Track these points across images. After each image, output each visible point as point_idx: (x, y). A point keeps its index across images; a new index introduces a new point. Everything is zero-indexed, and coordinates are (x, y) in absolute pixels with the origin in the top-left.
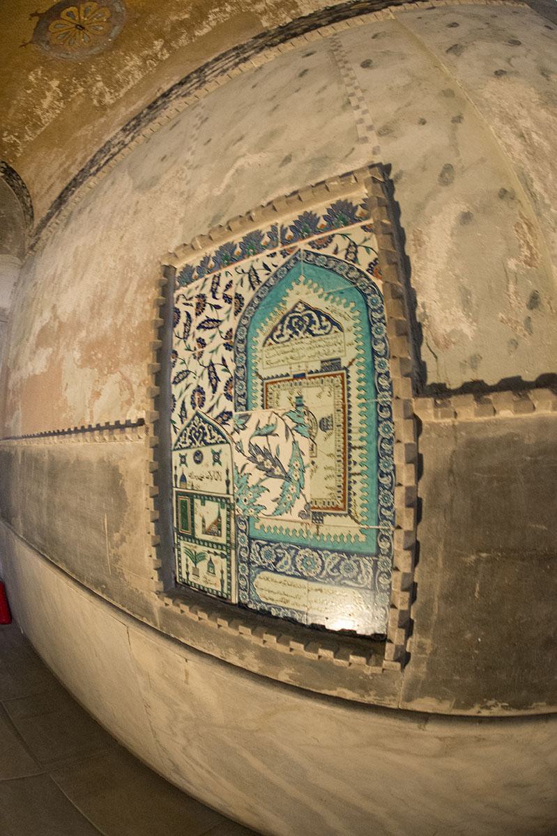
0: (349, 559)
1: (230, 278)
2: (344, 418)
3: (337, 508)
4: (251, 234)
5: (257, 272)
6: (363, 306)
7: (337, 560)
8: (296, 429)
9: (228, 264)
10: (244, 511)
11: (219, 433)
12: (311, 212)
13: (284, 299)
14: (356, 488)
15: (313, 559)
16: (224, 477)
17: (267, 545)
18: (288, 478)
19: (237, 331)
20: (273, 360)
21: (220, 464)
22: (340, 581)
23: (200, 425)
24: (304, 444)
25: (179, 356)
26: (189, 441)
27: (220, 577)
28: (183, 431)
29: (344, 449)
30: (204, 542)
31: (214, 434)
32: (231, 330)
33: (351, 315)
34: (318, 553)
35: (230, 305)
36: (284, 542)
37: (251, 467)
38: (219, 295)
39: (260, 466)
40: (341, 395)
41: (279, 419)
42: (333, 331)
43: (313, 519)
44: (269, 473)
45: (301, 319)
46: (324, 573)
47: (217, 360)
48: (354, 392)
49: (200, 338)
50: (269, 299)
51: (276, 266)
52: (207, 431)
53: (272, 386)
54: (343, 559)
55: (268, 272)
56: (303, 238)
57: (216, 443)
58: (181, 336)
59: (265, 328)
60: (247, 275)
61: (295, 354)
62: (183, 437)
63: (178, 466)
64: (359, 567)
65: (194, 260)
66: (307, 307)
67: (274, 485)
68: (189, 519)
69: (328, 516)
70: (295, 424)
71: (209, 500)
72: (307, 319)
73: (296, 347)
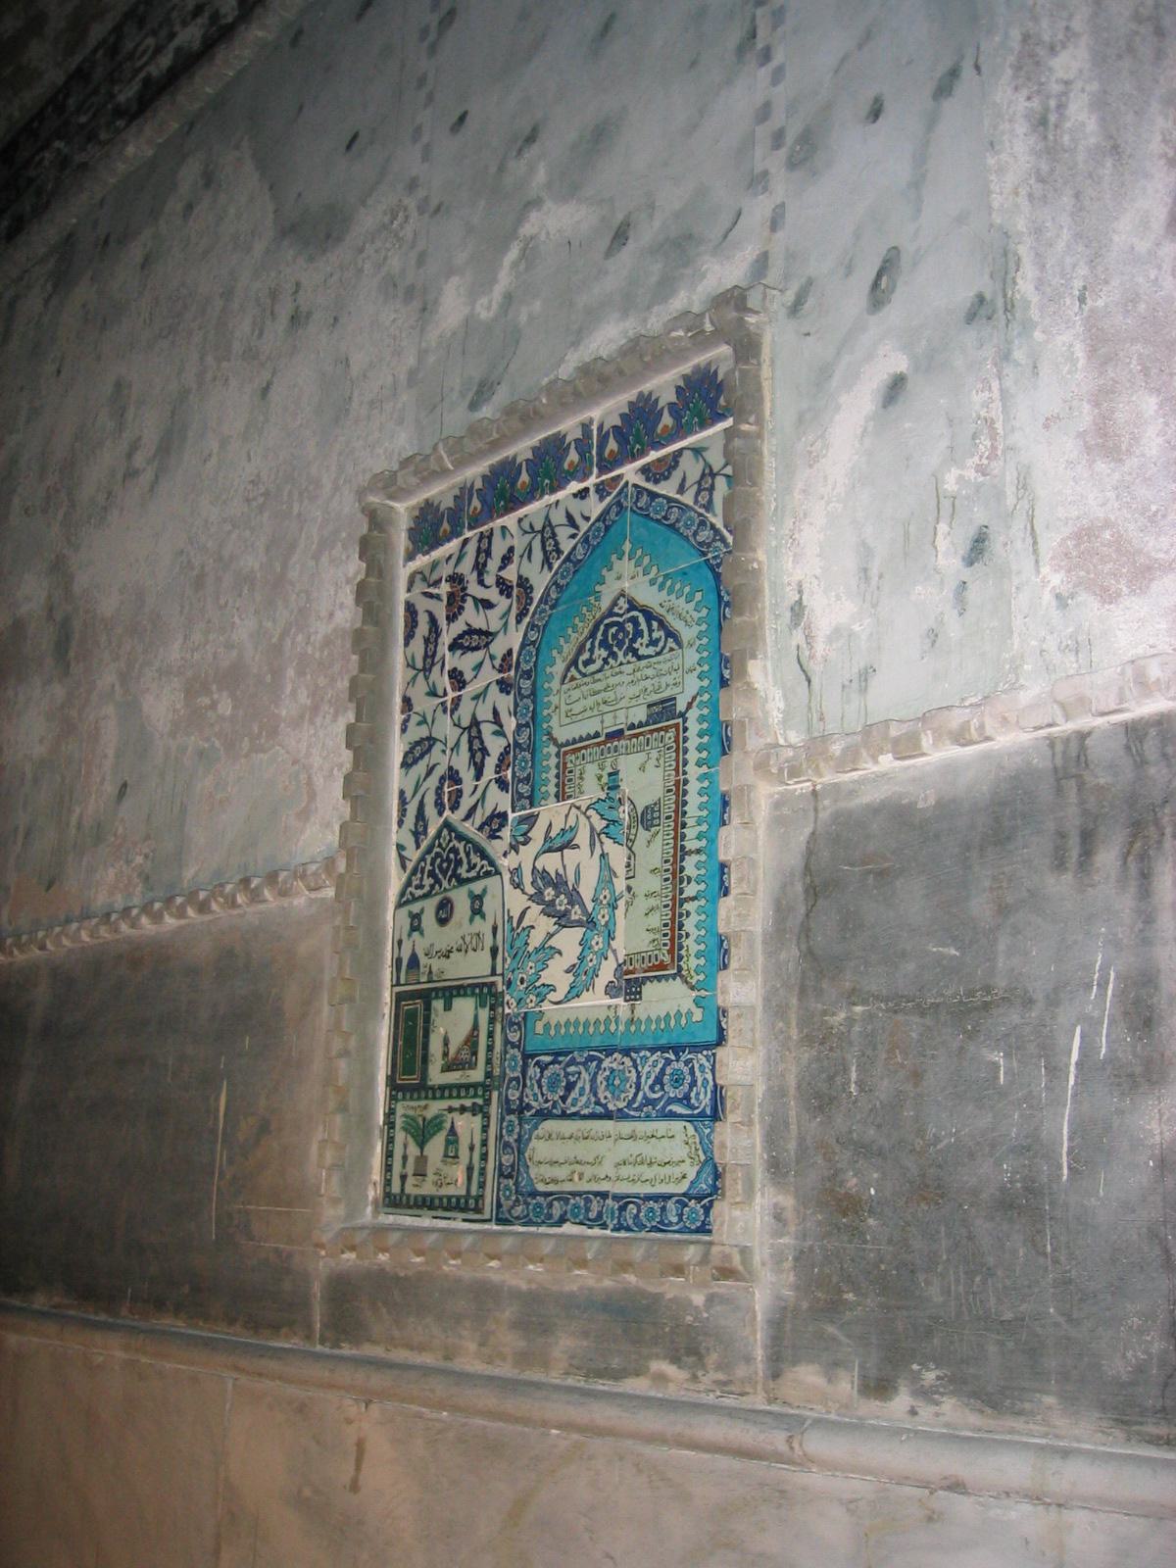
0: (677, 1061)
1: (508, 542)
2: (676, 802)
3: (662, 967)
4: (546, 439)
5: (557, 530)
6: (713, 597)
7: (660, 1066)
8: (606, 830)
9: (508, 510)
10: (519, 1002)
11: (484, 855)
12: (650, 394)
13: (598, 588)
14: (689, 925)
15: (623, 1071)
16: (488, 942)
17: (552, 1063)
18: (590, 923)
19: (519, 654)
20: (577, 708)
21: (483, 917)
22: (664, 1108)
23: (451, 845)
24: (618, 855)
25: (417, 708)
26: (428, 882)
27: (467, 1161)
28: (419, 862)
29: (675, 855)
30: (444, 1091)
31: (475, 859)
32: (510, 652)
33: (696, 615)
34: (632, 1059)
35: (509, 601)
36: (581, 1049)
37: (536, 909)
38: (490, 579)
39: (549, 910)
40: (674, 763)
41: (582, 818)
42: (667, 649)
43: (626, 994)
44: (563, 920)
45: (621, 626)
46: (641, 1094)
47: (484, 713)
48: (693, 756)
49: (455, 669)
50: (573, 588)
51: (587, 519)
52: (462, 855)
53: (573, 757)
54: (668, 1062)
55: (575, 531)
56: (634, 458)
57: (478, 878)
58: (419, 664)
59: (566, 649)
60: (539, 536)
61: (610, 695)
62: (419, 875)
63: (404, 938)
64: (692, 1072)
65: (442, 493)
66: (633, 605)
67: (569, 941)
68: (419, 1047)
69: (648, 983)
70: (604, 823)
71: (459, 995)
72: (629, 627)
73: (612, 681)
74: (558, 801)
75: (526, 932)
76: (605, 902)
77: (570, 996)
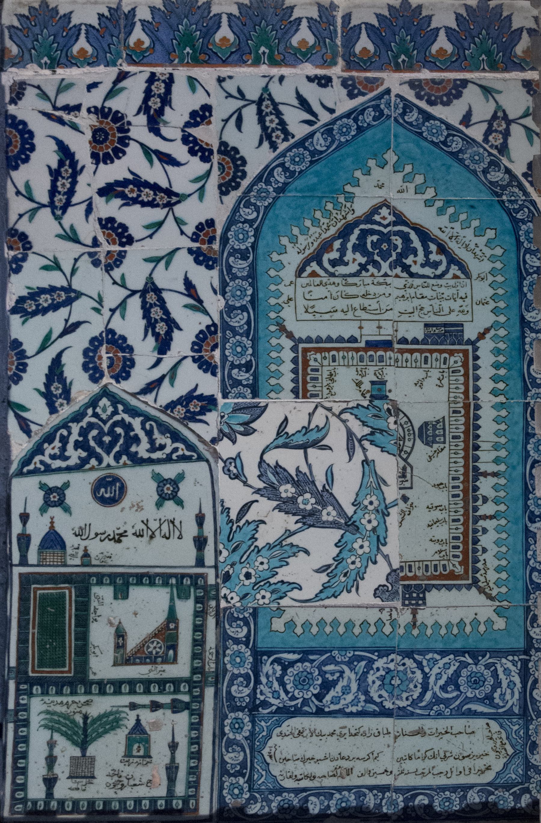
0: (476, 664)
7: (453, 668)
15: (405, 672)
34: (415, 660)
36: (345, 649)
43: (404, 599)
46: (428, 696)
54: (464, 665)
74: (297, 397)
75: (252, 526)
76: (371, 508)
77: (323, 596)
